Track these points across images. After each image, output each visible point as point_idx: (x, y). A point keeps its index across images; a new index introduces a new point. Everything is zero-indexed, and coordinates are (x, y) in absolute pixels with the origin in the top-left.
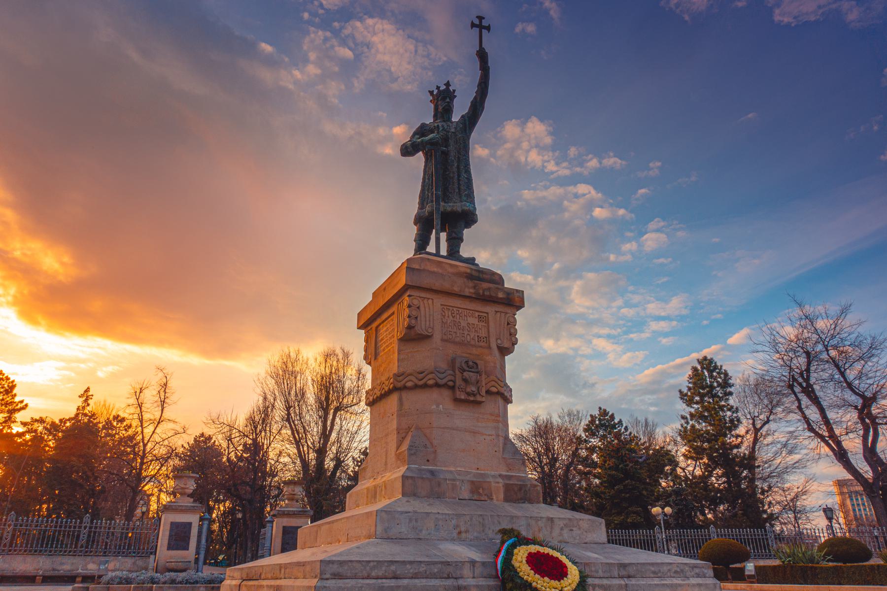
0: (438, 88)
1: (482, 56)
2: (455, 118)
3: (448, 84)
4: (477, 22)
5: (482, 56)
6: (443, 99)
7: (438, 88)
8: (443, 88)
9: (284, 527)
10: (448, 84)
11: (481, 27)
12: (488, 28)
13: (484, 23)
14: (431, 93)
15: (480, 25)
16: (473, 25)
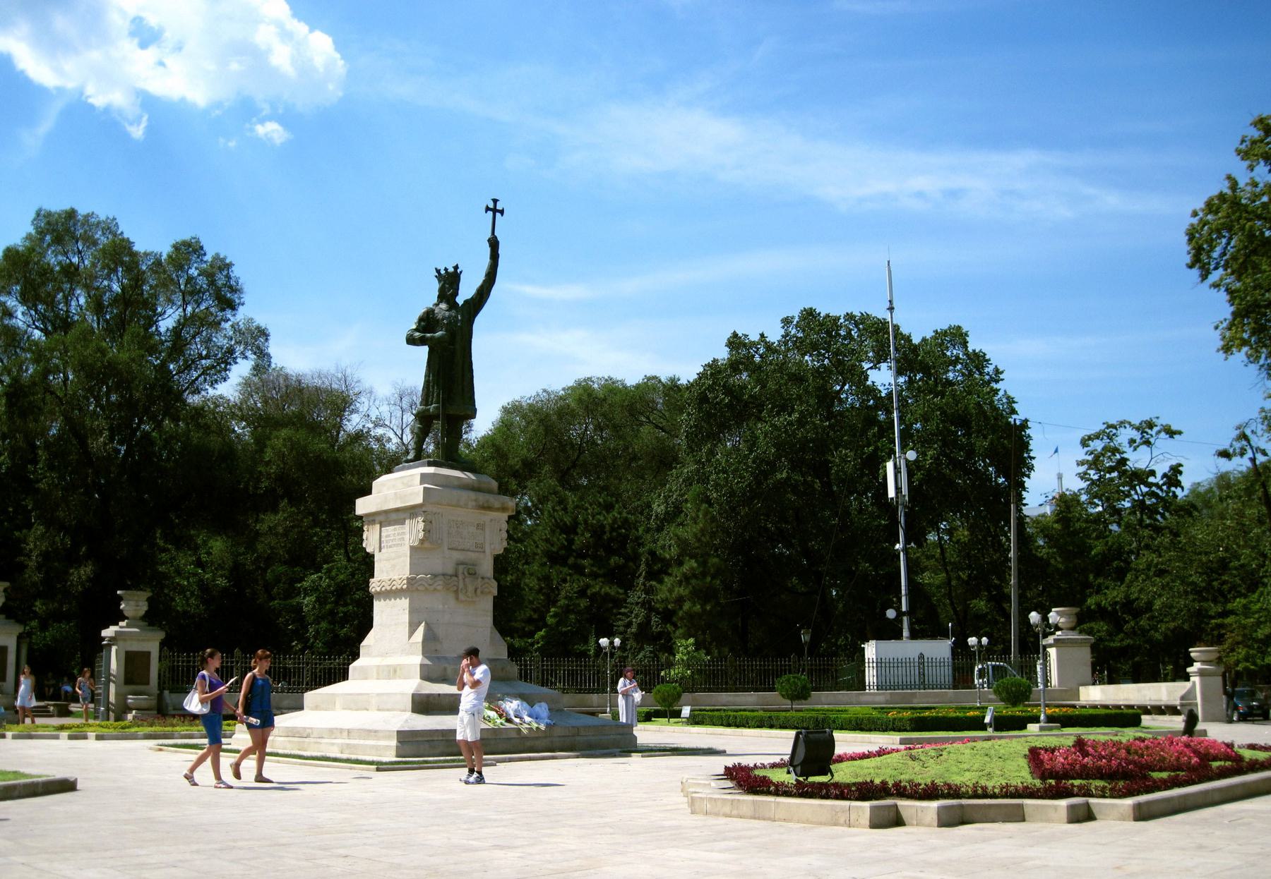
0: (446, 269)
1: (494, 244)
2: (460, 301)
3: (456, 268)
4: (491, 206)
5: (494, 244)
6: (450, 281)
7: (446, 269)
8: (451, 270)
9: (127, 652)
10: (456, 268)
11: (495, 211)
12: (502, 212)
13: (499, 207)
14: (438, 271)
15: (495, 210)
16: (488, 209)
